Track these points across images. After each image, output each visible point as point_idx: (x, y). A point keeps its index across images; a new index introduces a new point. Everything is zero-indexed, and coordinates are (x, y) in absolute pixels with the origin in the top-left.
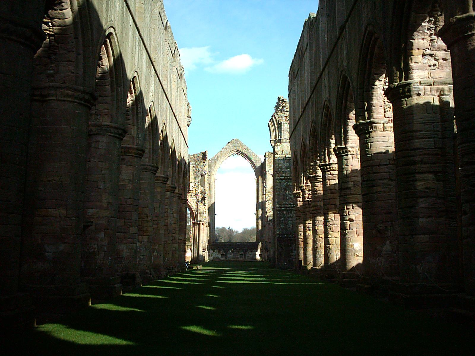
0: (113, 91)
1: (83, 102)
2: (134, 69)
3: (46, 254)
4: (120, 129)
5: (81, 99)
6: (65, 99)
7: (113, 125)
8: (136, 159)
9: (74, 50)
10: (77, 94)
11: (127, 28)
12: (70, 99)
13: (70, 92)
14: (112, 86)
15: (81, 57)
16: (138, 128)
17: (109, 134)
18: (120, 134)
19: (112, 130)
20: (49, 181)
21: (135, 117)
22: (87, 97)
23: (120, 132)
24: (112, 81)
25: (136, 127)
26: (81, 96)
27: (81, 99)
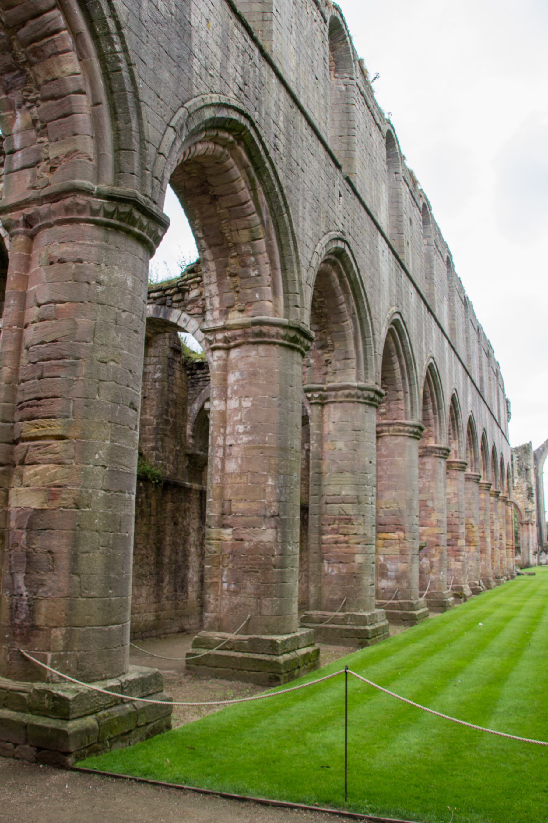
0: (435, 414)
1: (412, 435)
2: (452, 387)
3: (389, 573)
4: (444, 449)
5: (411, 433)
6: (397, 434)
7: (438, 445)
8: (459, 473)
9: (402, 389)
10: (406, 428)
11: (443, 351)
12: (402, 434)
13: (402, 428)
14: (434, 409)
15: (408, 395)
16: (459, 442)
17: (434, 454)
18: (445, 454)
19: (437, 451)
20: (387, 508)
21: (456, 432)
22: (416, 430)
23: (445, 452)
24: (434, 405)
25: (457, 441)
26: (411, 429)
27: (411, 433)
